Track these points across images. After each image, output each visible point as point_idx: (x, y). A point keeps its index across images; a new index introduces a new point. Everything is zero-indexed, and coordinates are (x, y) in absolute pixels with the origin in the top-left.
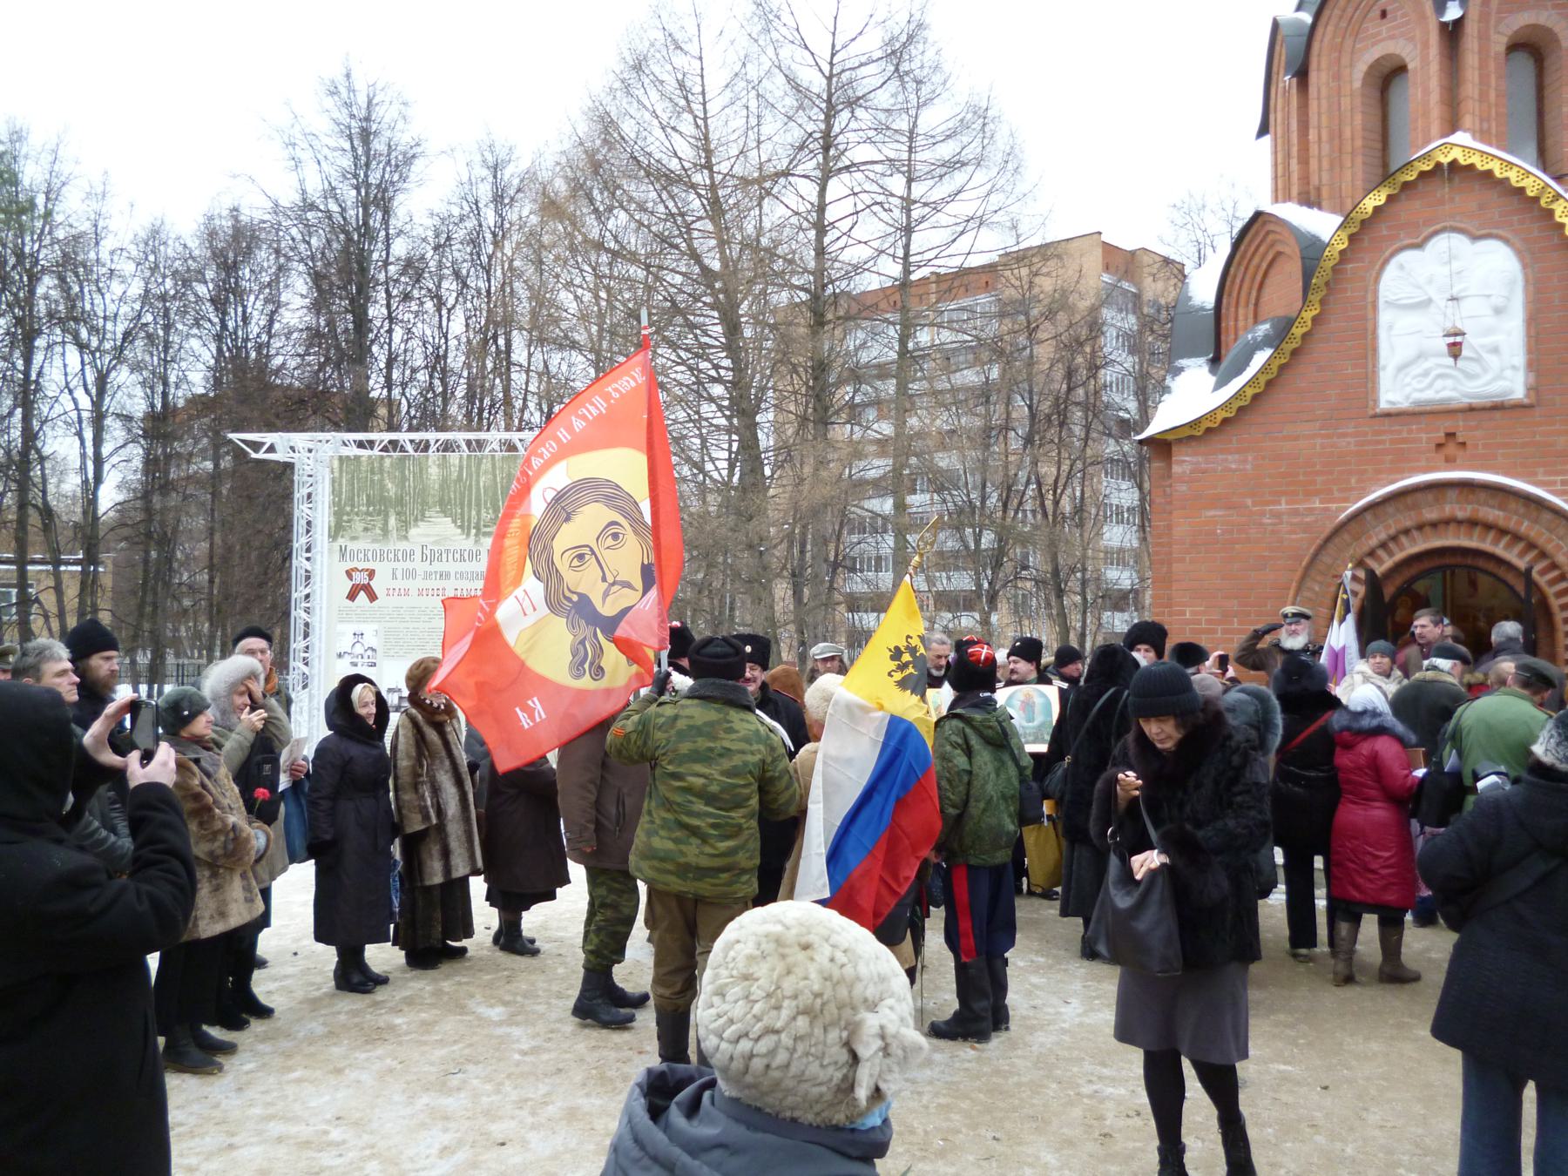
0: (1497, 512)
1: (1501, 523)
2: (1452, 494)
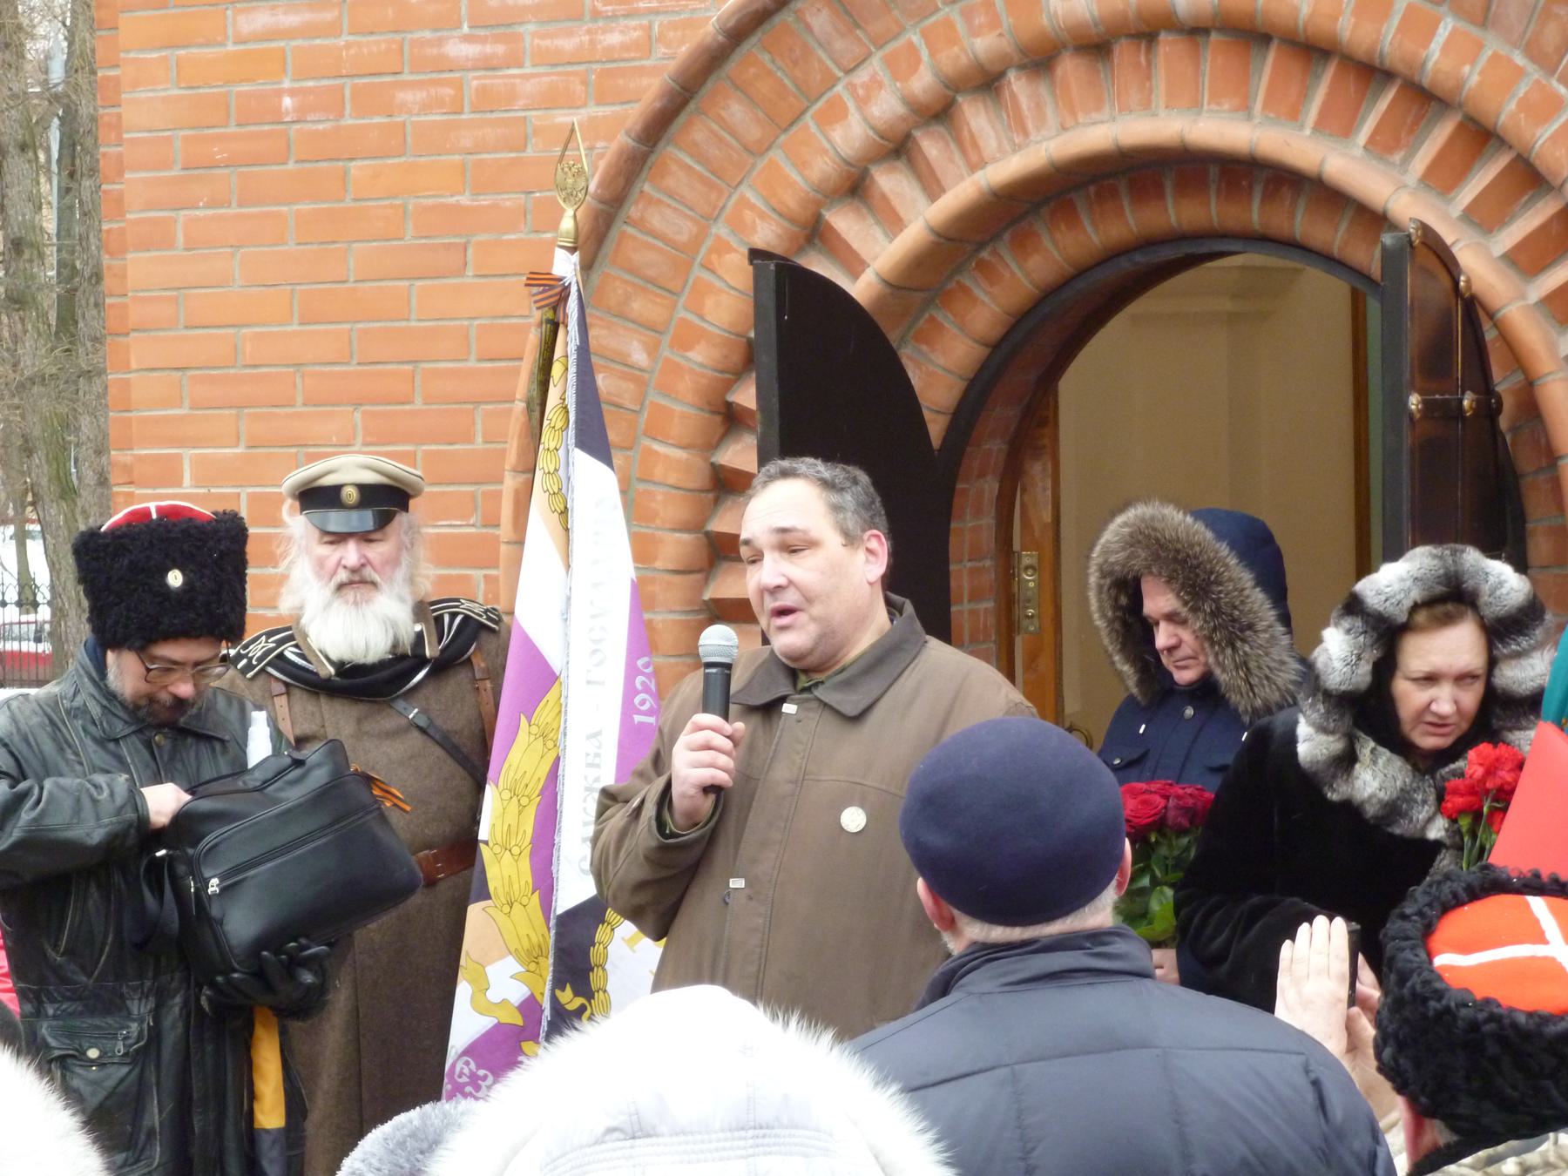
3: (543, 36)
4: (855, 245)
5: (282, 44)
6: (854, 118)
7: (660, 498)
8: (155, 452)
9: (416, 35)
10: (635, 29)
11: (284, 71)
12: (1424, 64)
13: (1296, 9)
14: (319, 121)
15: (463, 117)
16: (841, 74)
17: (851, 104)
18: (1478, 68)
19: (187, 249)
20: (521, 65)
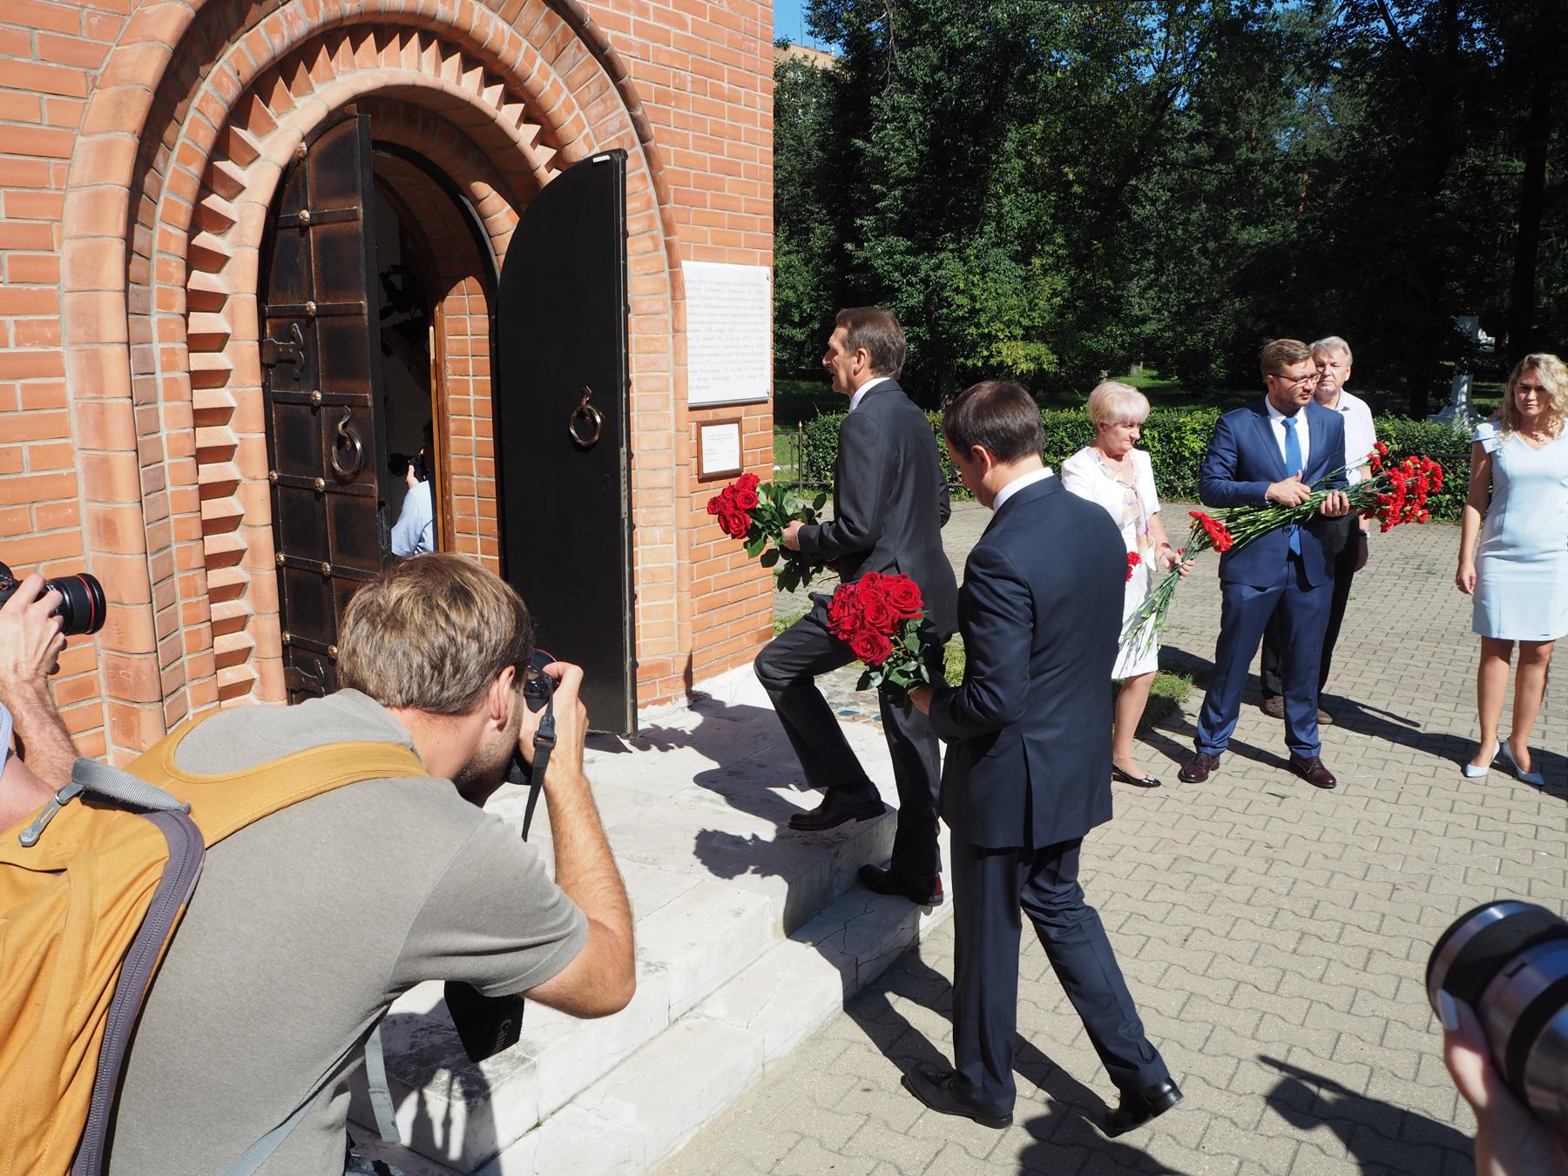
1: (506, 52)
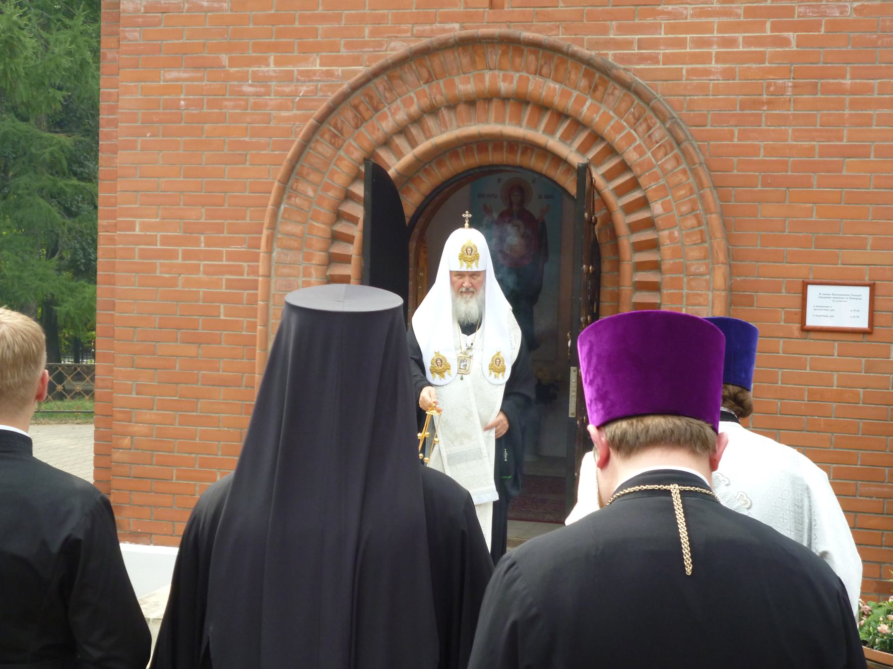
0: (552, 84)
1: (557, 100)
2: (494, 56)
3: (279, 86)
4: (386, 160)
5: (181, 83)
6: (390, 119)
7: (315, 240)
8: (126, 219)
9: (232, 83)
10: (312, 86)
11: (182, 93)
12: (581, 113)
13: (541, 94)
14: (194, 110)
15: (248, 111)
16: (386, 105)
17: (389, 114)
18: (599, 115)
19: (141, 150)
20: (269, 95)
